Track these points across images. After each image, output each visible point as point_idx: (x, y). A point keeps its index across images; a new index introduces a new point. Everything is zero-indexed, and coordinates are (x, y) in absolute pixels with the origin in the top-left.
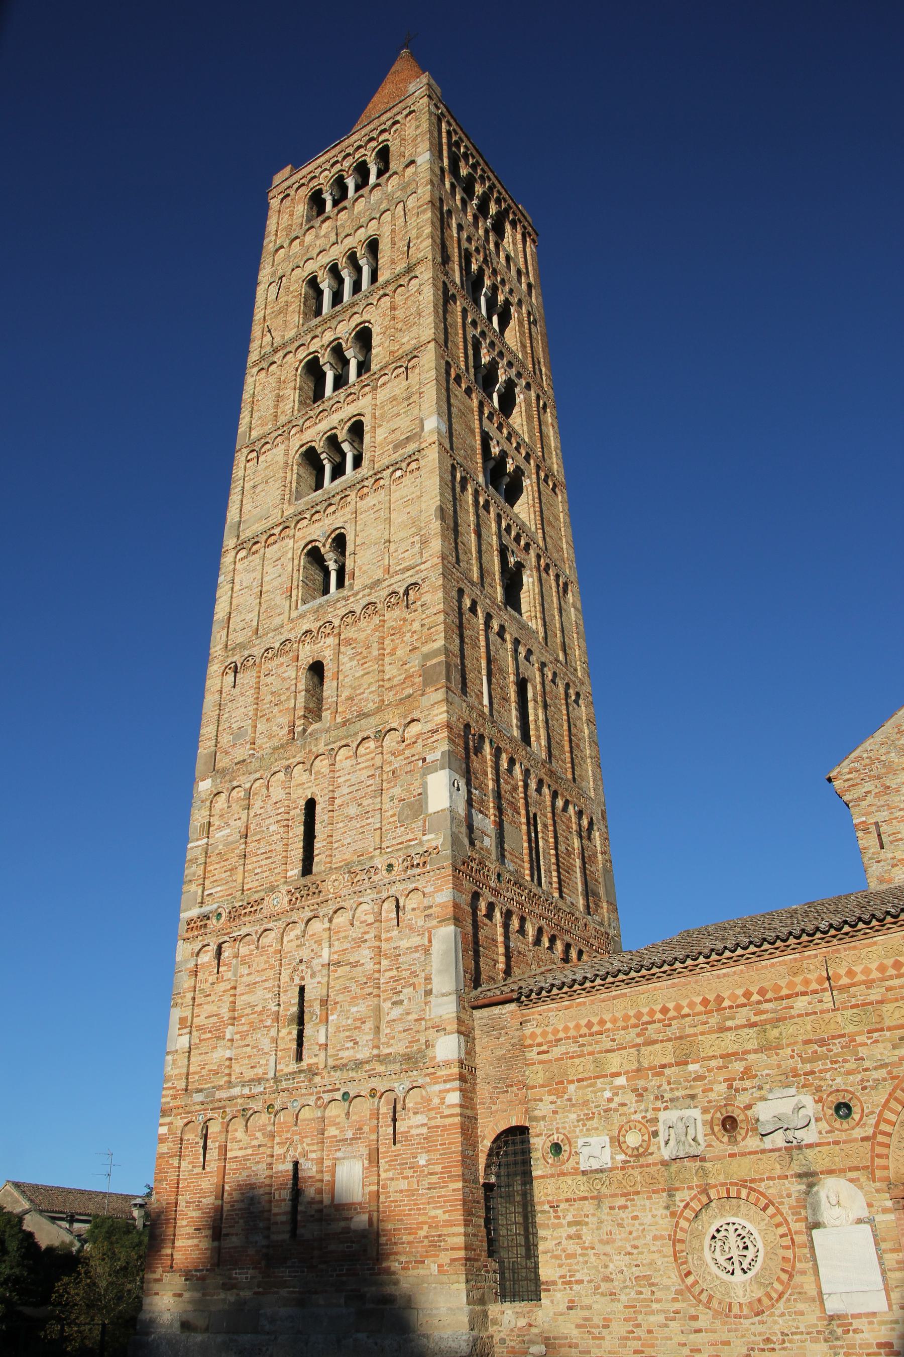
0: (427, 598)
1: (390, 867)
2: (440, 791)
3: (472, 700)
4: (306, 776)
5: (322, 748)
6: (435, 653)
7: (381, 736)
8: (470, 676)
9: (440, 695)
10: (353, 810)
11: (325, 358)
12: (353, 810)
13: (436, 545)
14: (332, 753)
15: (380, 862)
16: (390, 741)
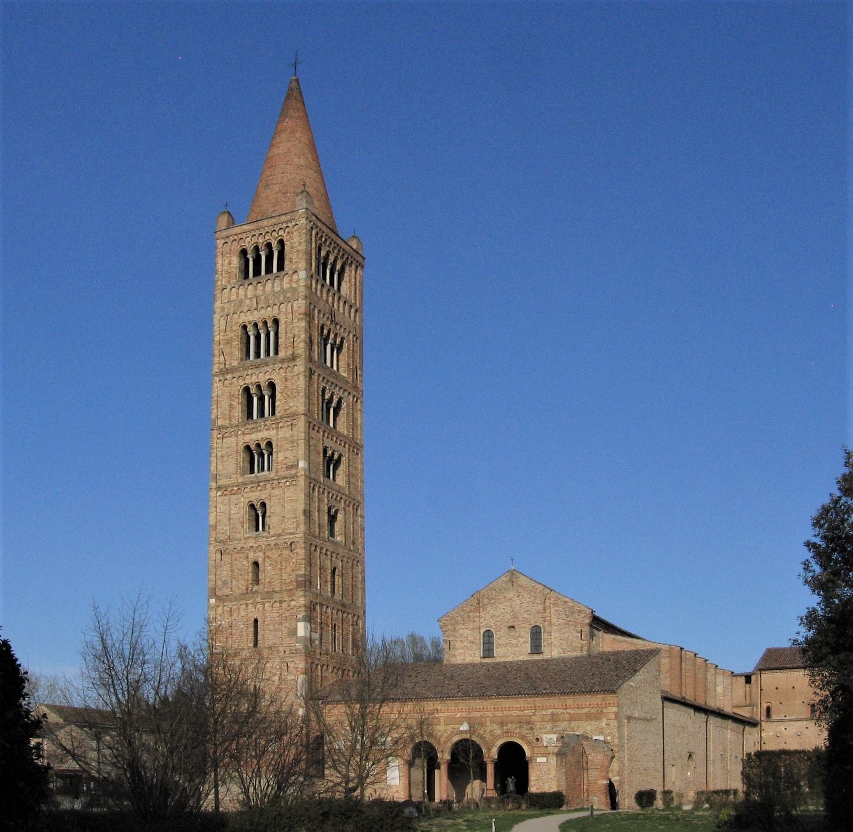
0: (298, 550)
1: (285, 652)
2: (302, 629)
3: (314, 590)
4: (253, 609)
5: (259, 600)
6: (300, 576)
7: (281, 602)
8: (313, 580)
9: (302, 593)
10: (271, 627)
11: (253, 390)
12: (271, 627)
13: (302, 528)
14: (263, 604)
15: (281, 649)
16: (284, 605)
